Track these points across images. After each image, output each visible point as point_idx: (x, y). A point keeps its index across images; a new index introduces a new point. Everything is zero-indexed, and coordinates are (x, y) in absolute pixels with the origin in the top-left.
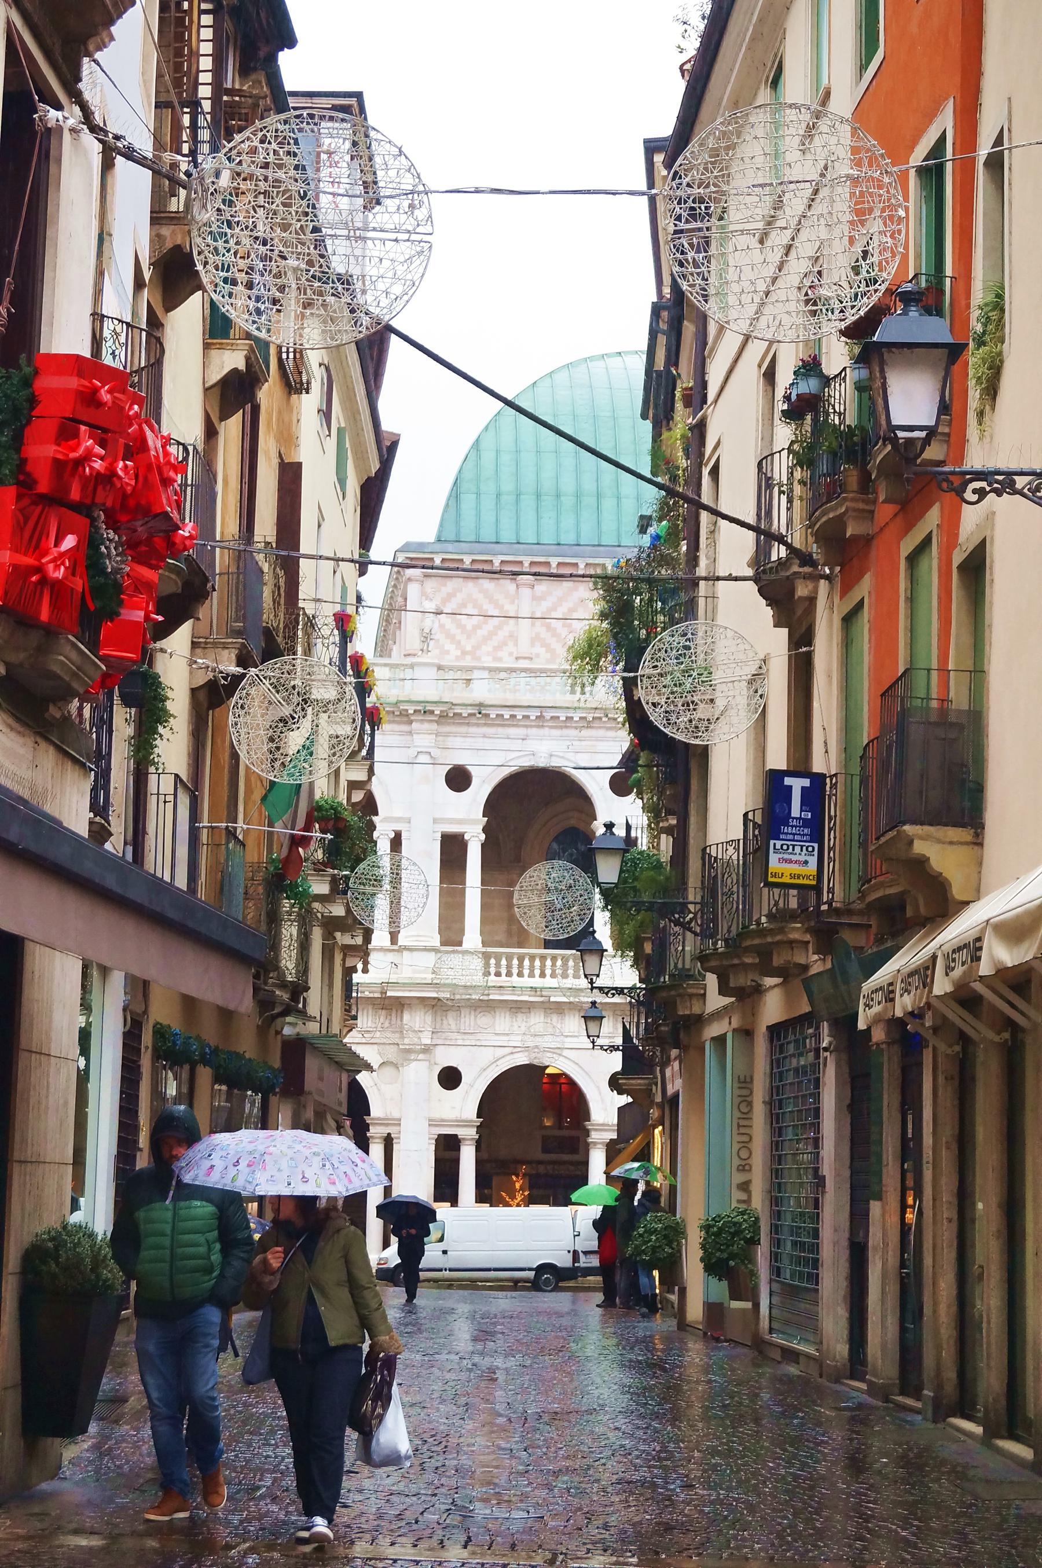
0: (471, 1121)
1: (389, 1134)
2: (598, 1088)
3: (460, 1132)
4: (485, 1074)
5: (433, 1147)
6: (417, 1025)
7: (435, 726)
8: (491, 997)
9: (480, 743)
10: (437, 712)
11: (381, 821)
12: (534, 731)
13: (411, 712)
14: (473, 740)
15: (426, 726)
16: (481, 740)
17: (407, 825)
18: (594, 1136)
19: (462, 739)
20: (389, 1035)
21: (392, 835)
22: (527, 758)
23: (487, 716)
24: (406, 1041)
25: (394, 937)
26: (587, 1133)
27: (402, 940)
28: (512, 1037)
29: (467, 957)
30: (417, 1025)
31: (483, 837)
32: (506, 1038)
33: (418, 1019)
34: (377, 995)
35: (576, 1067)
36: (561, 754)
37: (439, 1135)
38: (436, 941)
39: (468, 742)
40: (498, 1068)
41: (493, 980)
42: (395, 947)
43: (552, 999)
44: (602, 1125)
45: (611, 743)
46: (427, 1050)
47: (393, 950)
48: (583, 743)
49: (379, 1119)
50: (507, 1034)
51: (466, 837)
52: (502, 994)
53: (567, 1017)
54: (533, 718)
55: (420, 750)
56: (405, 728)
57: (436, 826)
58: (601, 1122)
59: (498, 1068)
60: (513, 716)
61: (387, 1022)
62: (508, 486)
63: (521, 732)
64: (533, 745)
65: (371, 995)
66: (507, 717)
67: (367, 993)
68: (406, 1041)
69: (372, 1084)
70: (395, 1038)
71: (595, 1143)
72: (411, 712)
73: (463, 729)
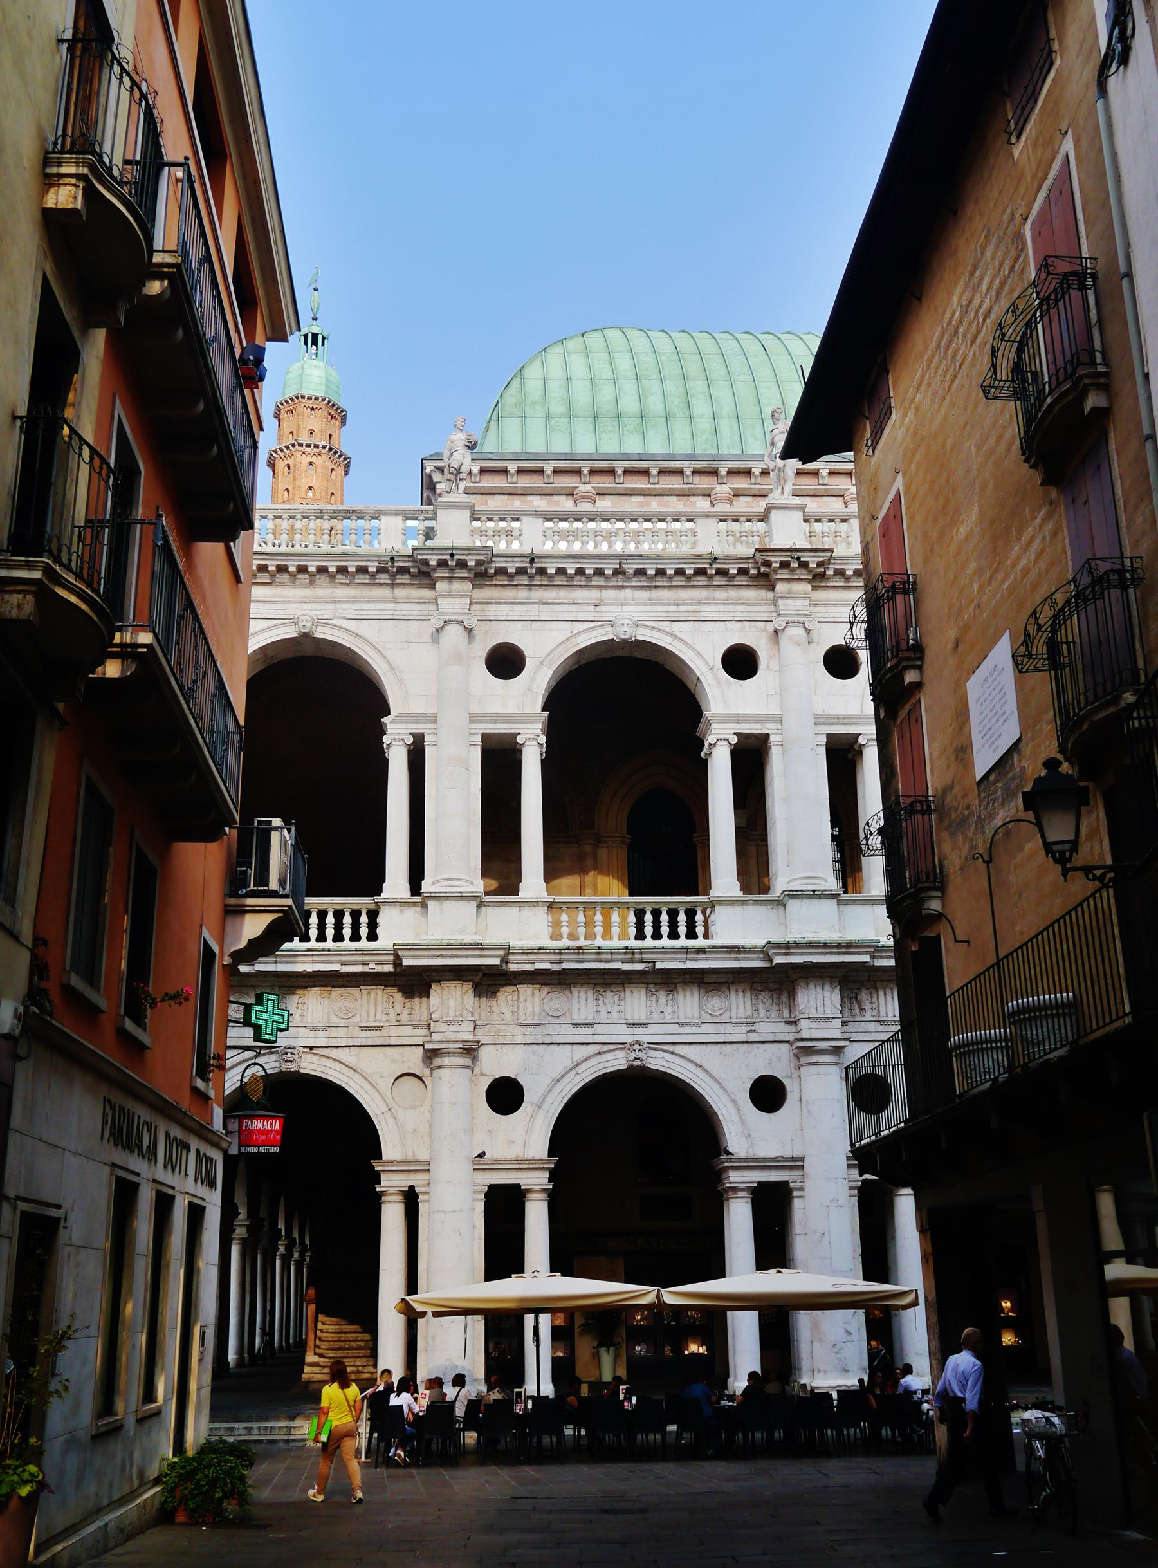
0: (542, 1161)
1: (412, 1188)
2: (734, 1101)
3: (525, 1179)
4: (560, 1086)
5: (480, 1207)
6: (452, 1013)
7: (468, 586)
8: (565, 966)
9: (534, 611)
10: (471, 563)
11: (393, 721)
12: (610, 594)
13: (433, 563)
14: (524, 608)
15: (457, 586)
16: (536, 607)
17: (432, 726)
18: (735, 1178)
19: (508, 607)
20: (408, 1030)
21: (410, 740)
22: (602, 631)
23: (542, 572)
24: (435, 1037)
25: (415, 889)
26: (718, 1176)
27: (426, 886)
28: (599, 1029)
29: (527, 911)
30: (452, 1013)
31: (543, 739)
32: (589, 1030)
33: (452, 1003)
34: (389, 968)
35: (699, 1072)
36: (652, 624)
37: (491, 1187)
38: (478, 885)
39: (518, 611)
40: (578, 1078)
41: (565, 942)
42: (418, 899)
43: (659, 966)
44: (746, 1160)
45: (722, 608)
46: (470, 1051)
47: (414, 904)
48: (682, 608)
49: (393, 1162)
50: (592, 1025)
51: (519, 740)
52: (582, 961)
53: (681, 996)
54: (609, 572)
55: (447, 618)
56: (426, 593)
57: (473, 726)
58: (743, 1155)
59: (578, 1078)
60: (580, 572)
61: (406, 1012)
62: (557, 408)
63: (592, 595)
64: (609, 612)
65: (379, 969)
66: (571, 571)
67: (372, 965)
68: (435, 1037)
69: (385, 1109)
70: (419, 1036)
71: (735, 1190)
72: (433, 563)
73: (509, 593)
